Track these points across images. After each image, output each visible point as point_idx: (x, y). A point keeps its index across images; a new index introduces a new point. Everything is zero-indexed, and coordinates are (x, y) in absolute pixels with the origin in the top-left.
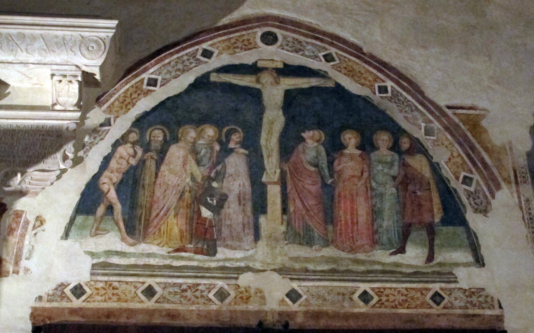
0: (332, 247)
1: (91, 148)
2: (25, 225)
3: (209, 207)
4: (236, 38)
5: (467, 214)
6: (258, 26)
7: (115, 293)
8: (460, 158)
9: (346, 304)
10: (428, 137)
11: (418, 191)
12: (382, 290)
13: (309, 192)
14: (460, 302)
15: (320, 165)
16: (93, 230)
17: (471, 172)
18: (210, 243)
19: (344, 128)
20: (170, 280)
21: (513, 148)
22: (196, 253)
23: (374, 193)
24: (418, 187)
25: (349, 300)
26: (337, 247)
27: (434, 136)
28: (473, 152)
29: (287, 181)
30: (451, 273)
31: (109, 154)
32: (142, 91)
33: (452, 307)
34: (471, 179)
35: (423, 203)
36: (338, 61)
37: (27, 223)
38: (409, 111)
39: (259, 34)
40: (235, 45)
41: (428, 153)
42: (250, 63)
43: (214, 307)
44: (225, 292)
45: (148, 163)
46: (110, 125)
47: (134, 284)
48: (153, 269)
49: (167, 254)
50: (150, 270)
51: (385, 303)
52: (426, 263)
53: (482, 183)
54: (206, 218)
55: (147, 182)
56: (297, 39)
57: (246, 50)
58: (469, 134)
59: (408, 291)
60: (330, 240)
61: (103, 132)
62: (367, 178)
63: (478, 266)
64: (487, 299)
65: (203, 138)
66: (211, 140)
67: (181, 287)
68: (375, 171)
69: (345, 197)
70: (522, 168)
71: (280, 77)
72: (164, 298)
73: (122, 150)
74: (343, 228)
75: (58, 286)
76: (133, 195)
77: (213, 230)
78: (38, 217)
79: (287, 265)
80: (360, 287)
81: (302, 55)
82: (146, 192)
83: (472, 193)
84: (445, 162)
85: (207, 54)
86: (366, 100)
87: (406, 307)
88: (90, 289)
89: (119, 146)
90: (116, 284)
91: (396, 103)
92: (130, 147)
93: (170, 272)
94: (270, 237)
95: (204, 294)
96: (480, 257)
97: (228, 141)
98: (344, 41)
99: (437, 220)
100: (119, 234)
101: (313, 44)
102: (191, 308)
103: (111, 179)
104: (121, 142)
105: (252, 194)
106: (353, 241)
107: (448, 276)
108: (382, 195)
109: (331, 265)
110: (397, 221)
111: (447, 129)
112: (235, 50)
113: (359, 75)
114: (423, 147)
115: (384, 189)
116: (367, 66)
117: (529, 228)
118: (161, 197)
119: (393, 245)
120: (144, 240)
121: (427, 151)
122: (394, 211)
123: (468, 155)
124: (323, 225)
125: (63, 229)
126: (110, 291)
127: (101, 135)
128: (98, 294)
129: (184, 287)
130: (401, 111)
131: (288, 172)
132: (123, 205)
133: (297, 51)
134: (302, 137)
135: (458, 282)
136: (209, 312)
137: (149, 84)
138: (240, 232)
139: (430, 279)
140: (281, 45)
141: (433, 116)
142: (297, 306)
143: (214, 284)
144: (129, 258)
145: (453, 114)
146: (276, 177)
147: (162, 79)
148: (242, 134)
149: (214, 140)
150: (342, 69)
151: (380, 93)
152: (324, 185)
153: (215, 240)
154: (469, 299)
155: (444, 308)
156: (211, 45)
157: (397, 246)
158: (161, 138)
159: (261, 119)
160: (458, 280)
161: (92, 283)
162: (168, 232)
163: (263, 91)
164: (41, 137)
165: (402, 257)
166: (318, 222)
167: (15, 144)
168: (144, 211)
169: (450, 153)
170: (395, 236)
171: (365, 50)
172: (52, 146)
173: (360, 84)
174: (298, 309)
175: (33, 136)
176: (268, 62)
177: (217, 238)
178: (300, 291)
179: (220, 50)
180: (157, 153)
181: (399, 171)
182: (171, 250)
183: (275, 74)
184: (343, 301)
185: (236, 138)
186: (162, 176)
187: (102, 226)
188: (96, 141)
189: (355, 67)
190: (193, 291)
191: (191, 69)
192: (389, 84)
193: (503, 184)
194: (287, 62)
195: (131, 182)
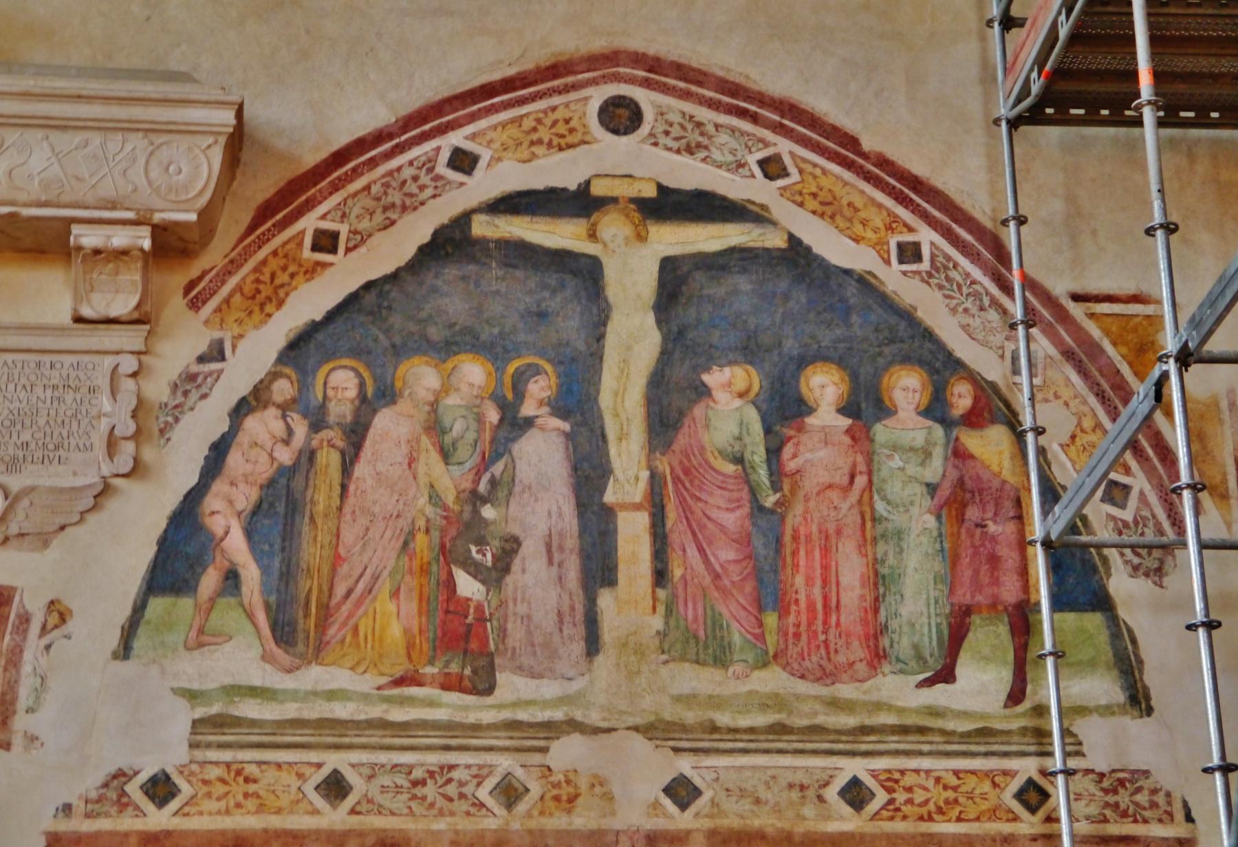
0: (777, 669)
1: (177, 420)
2: (21, 623)
3: (475, 570)
5: (1111, 580)
6: (594, 82)
7: (250, 792)
9: (809, 811)
11: (990, 523)
12: (897, 776)
13: (722, 528)
14: (1087, 805)
15: (747, 456)
16: (193, 634)
18: (482, 662)
20: (383, 757)
22: (445, 687)
24: (990, 515)
25: (817, 802)
31: (223, 435)
32: (300, 265)
34: (1126, 489)
36: (795, 177)
37: (25, 619)
38: (974, 310)
39: (594, 106)
40: (535, 137)
42: (573, 187)
43: (491, 823)
44: (517, 785)
46: (223, 359)
47: (295, 767)
48: (344, 732)
49: (375, 692)
50: (333, 732)
51: (903, 808)
52: (1006, 706)
53: (1153, 498)
54: (469, 599)
55: (321, 507)
56: (691, 117)
57: (561, 149)
59: (959, 778)
60: (771, 653)
61: (206, 378)
62: (864, 491)
63: (1136, 713)
64: (1155, 798)
65: (457, 390)
66: (476, 397)
67: (410, 773)
68: (884, 472)
69: (808, 538)
71: (648, 222)
72: (370, 801)
74: (804, 618)
75: (109, 778)
76: (287, 544)
77: (485, 629)
78: (52, 602)
79: (667, 716)
80: (841, 769)
81: (704, 160)
82: (320, 533)
83: (1126, 524)
84: (1062, 446)
85: (463, 161)
87: (954, 818)
88: (189, 782)
89: (246, 415)
90: (251, 770)
91: (941, 287)
92: (276, 418)
93: (385, 736)
94: (625, 645)
95: (467, 790)
96: (1141, 691)
98: (813, 121)
101: (733, 130)
103: (231, 503)
104: (254, 403)
105: (581, 536)
106: (828, 653)
108: (899, 534)
109: (773, 713)
110: (936, 602)
111: (1068, 355)
112: (534, 149)
113: (848, 212)
118: (357, 548)
119: (926, 662)
120: (317, 657)
122: (931, 577)
124: (755, 612)
125: (118, 633)
126: (239, 788)
127: (199, 386)
128: (209, 795)
129: (418, 774)
130: (954, 311)
131: (669, 478)
132: (265, 570)
133: (690, 150)
135: (1084, 755)
137: (315, 248)
138: (551, 634)
139: (1014, 748)
140: (651, 135)
142: (691, 818)
143: (491, 766)
144: (282, 702)
145: (1086, 314)
146: (638, 492)
147: (350, 231)
148: (554, 380)
149: (484, 395)
150: (807, 197)
151: (901, 262)
153: (491, 655)
154: (1111, 799)
156: (473, 137)
157: (936, 664)
158: (352, 393)
159: (600, 338)
160: (1085, 749)
161: (194, 767)
162: (377, 636)
163: (604, 260)
164: (49, 392)
165: (946, 691)
166: (744, 608)
168: (315, 582)
169: (1075, 421)
170: (930, 638)
171: (867, 144)
172: (79, 416)
173: (850, 238)
174: (690, 826)
175: (29, 388)
176: (617, 181)
177: (497, 648)
178: (697, 781)
179: (496, 151)
180: (344, 433)
181: (945, 471)
182: (384, 680)
183: (637, 216)
184: (803, 804)
188: (190, 403)
190: (441, 781)
191: (422, 204)
192: (926, 237)
194: (665, 182)
195: (281, 508)
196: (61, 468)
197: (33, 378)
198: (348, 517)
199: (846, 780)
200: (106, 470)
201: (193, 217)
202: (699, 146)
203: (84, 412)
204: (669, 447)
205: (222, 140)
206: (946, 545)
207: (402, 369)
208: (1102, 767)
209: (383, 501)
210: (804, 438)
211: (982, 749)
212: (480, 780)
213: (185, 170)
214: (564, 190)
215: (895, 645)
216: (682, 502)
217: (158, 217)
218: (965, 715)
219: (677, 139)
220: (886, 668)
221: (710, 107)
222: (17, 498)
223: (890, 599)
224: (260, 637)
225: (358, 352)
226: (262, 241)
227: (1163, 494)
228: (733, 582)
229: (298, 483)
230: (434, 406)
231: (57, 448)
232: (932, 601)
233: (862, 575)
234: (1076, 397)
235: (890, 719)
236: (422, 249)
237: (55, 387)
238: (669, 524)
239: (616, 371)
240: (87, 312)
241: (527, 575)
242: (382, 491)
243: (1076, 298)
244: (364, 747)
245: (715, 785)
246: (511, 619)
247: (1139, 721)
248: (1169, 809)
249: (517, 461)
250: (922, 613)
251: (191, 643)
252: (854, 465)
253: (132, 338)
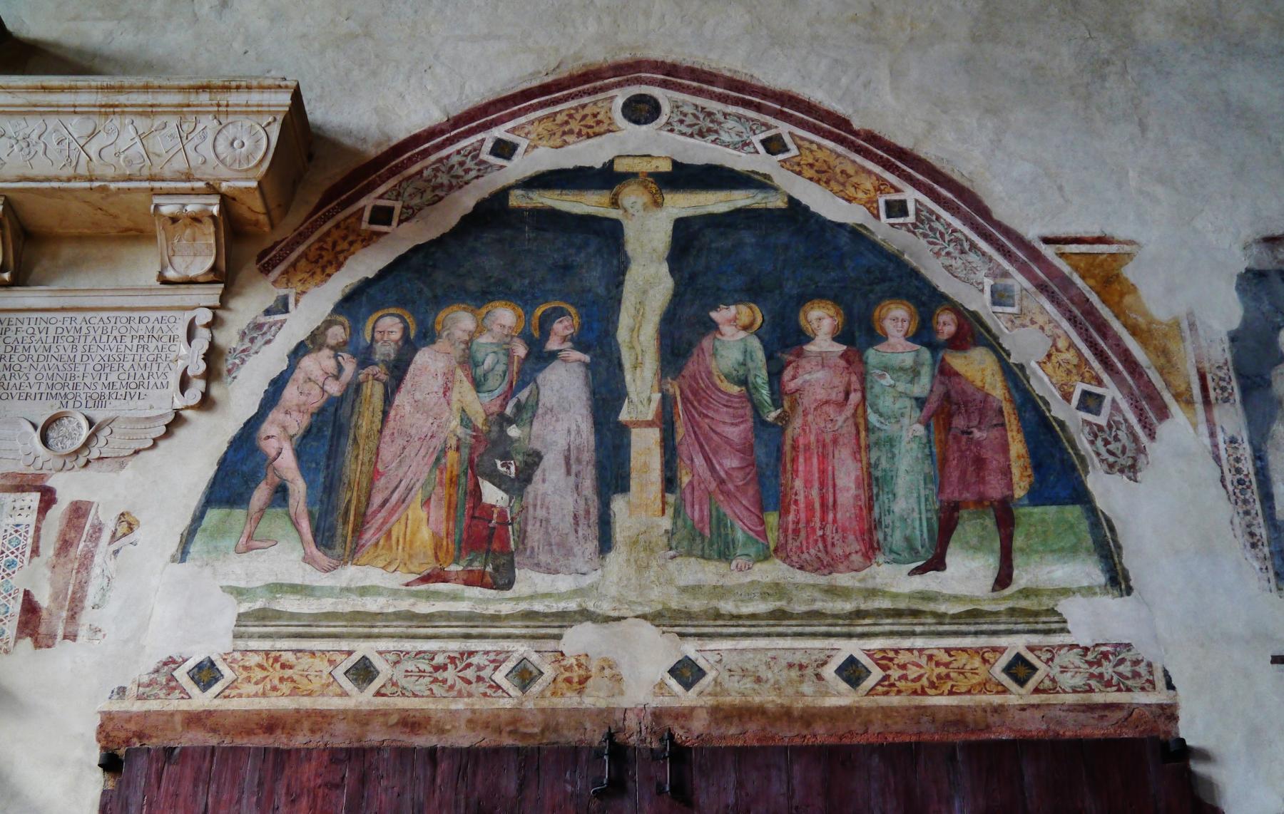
0: (778, 561)
1: (243, 361)
2: (95, 532)
4: (567, 112)
6: (619, 85)
7: (286, 677)
8: (1072, 352)
9: (807, 688)
11: (975, 430)
12: (891, 654)
13: (728, 441)
14: (1073, 677)
15: (751, 379)
16: (243, 540)
17: (1100, 383)
18: (502, 560)
19: (803, 299)
20: (408, 645)
21: (1198, 323)
22: (468, 583)
24: (975, 423)
25: (815, 680)
26: (786, 559)
27: (1013, 306)
28: (1104, 337)
29: (675, 418)
30: (1052, 612)
32: (359, 235)
33: (1054, 688)
34: (1100, 398)
35: (987, 454)
36: (794, 151)
37: (98, 529)
38: (956, 253)
39: (619, 102)
40: (566, 128)
41: (1000, 345)
42: (598, 165)
43: (506, 703)
44: (532, 668)
45: (366, 390)
46: (287, 311)
47: (328, 655)
49: (404, 588)
50: (365, 624)
51: (898, 683)
52: (994, 590)
53: (1124, 405)
54: (494, 506)
55: (363, 430)
56: (703, 108)
57: (589, 137)
58: (1094, 299)
59: (950, 656)
60: (772, 547)
61: (270, 327)
62: (858, 406)
63: (1116, 593)
64: (1137, 668)
66: (507, 336)
67: (433, 659)
68: (877, 389)
69: (807, 448)
70: (1219, 367)
71: (664, 191)
72: (394, 684)
74: (803, 515)
75: (160, 665)
76: (331, 462)
78: (123, 514)
81: (713, 142)
83: (1100, 428)
84: (1039, 363)
85: (504, 150)
86: (857, 234)
87: (946, 692)
88: (231, 668)
89: (303, 356)
90: (288, 657)
91: (925, 236)
93: (410, 627)
94: (635, 543)
97: (545, 333)
98: (809, 107)
99: (1019, 492)
100: (299, 546)
101: (739, 117)
102: (453, 707)
103: (284, 428)
104: (311, 346)
105: (597, 448)
107: (1044, 619)
108: (891, 442)
110: (927, 500)
111: (1042, 288)
114: (988, 330)
115: (896, 427)
116: (859, 159)
117: (1236, 503)
119: (918, 552)
120: (353, 558)
121: (996, 338)
123: (1093, 346)
124: (757, 512)
125: (178, 539)
126: (277, 673)
127: (265, 333)
128: (248, 679)
129: (440, 659)
130: (937, 254)
131: (679, 398)
132: (310, 485)
133: (701, 134)
134: (712, 320)
135: (1069, 632)
136: (496, 714)
139: (1002, 627)
140: (668, 123)
141: (1010, 261)
142: (695, 696)
144: (319, 598)
146: (650, 413)
147: (403, 207)
148: (576, 320)
151: (889, 216)
152: (760, 422)
154: (1095, 670)
155: (1037, 691)
156: (513, 130)
157: (926, 555)
158: (397, 335)
159: (620, 285)
160: (1069, 626)
161: (237, 655)
162: (408, 539)
163: (625, 222)
164: (136, 342)
165: (937, 578)
166: (747, 509)
167: (78, 359)
168: (355, 494)
169: (1051, 343)
170: (921, 531)
171: (856, 125)
172: (159, 360)
173: (843, 198)
174: (693, 704)
175: (119, 340)
176: (637, 160)
177: (517, 548)
178: (702, 663)
179: (532, 140)
180: (388, 368)
181: (932, 387)
183: (654, 187)
184: (801, 682)
185: (562, 327)
186: (398, 417)
187: (263, 527)
188: (255, 348)
189: (833, 161)
190: (460, 666)
191: (467, 183)
192: (911, 195)
193: (1174, 407)
194: (679, 160)
195: (328, 432)
196: (140, 402)
197: (123, 330)
198: (387, 439)
199: (843, 659)
200: (179, 404)
202: (709, 130)
203: (164, 358)
204: (680, 372)
205: (280, 118)
206: (935, 450)
208: (1086, 641)
209: (422, 425)
210: (803, 362)
211: (972, 628)
212: (497, 664)
213: (246, 144)
214: (591, 168)
215: (889, 538)
216: (691, 419)
217: (224, 186)
218: (956, 598)
219: (690, 126)
220: (881, 558)
221: (719, 100)
222: (99, 428)
223: (884, 497)
224: (302, 541)
225: (402, 303)
227: (1134, 402)
228: (737, 487)
229: (346, 408)
231: (138, 387)
232: (923, 500)
233: (857, 478)
234: (1050, 322)
235: (886, 604)
236: (465, 219)
237: (141, 337)
238: (678, 438)
239: (632, 311)
240: (171, 274)
241: (546, 485)
242: (418, 415)
243: (1047, 241)
244: (391, 636)
245: (718, 667)
246: (530, 522)
247: (1119, 600)
248: (1151, 678)
249: (541, 387)
250: (913, 510)
251: (241, 547)
252: (849, 384)
253: (211, 295)
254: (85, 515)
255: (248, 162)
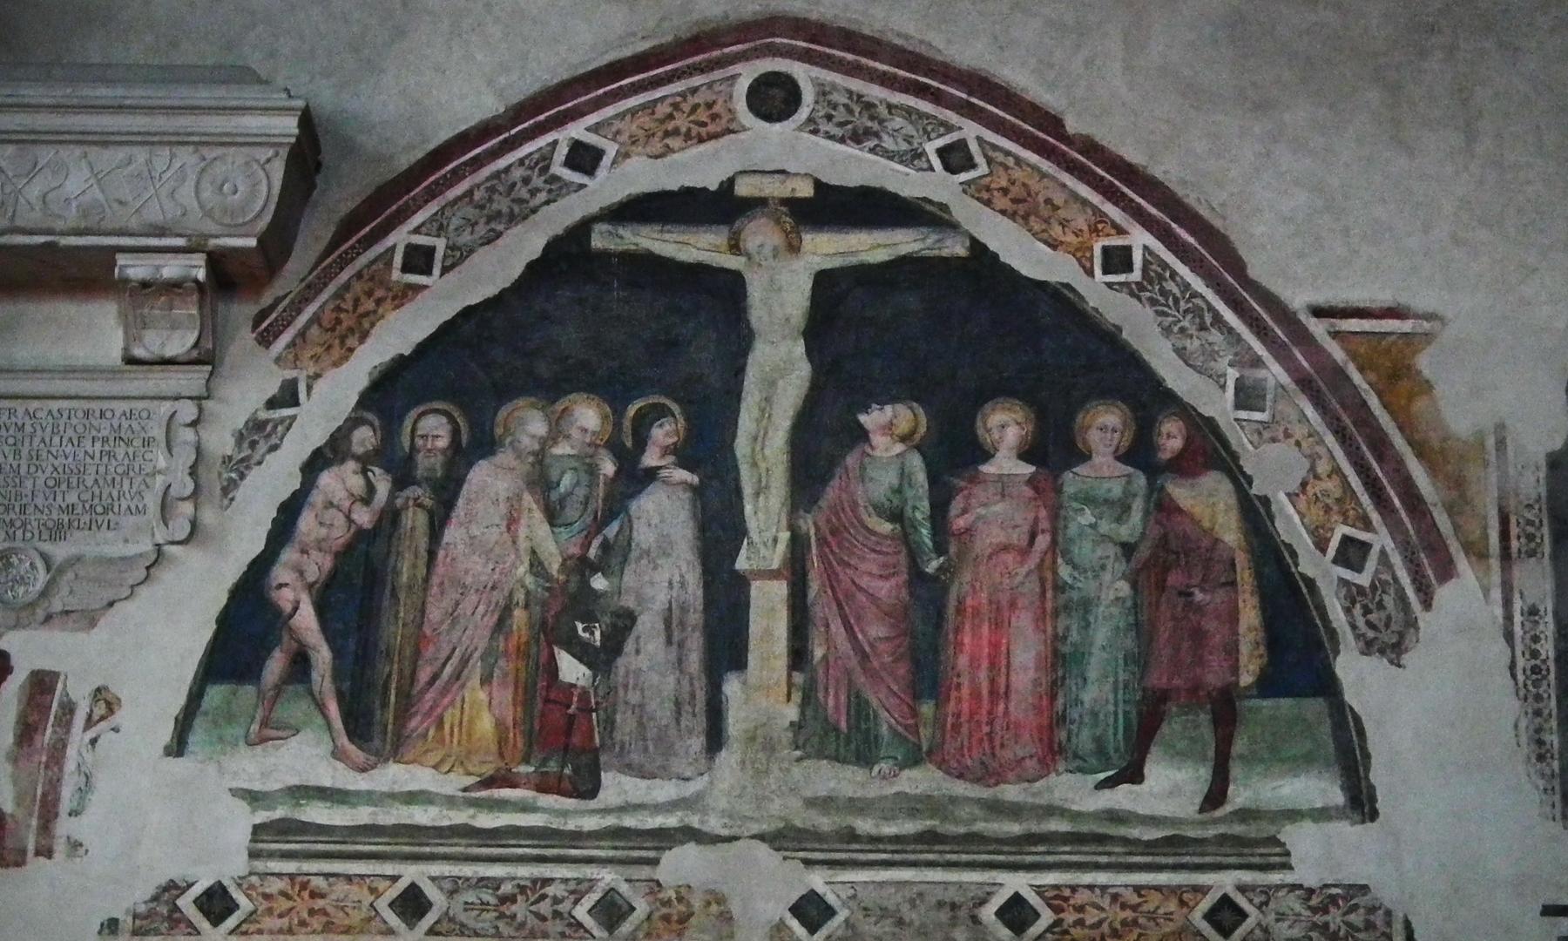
1: (242, 476)
2: (64, 714)
3: (583, 653)
4: (670, 101)
5: (1339, 659)
8: (1336, 479)
10: (1243, 414)
11: (1196, 591)
12: (1067, 893)
13: (872, 597)
14: (1290, 927)
15: (908, 511)
16: (255, 727)
17: (1367, 525)
18: (584, 759)
20: (467, 870)
21: (1508, 441)
22: (543, 788)
23: (1062, 599)
25: (970, 924)
26: (942, 765)
27: (1263, 410)
28: (1380, 459)
29: (809, 564)
30: (1274, 841)
31: (294, 494)
32: (389, 289)
34: (1365, 547)
35: (1210, 625)
37: (69, 709)
38: (1193, 331)
39: (743, 85)
40: (670, 126)
41: (1240, 468)
42: (713, 187)
44: (620, 902)
46: (296, 403)
47: (368, 881)
48: (425, 840)
49: (461, 794)
51: (1072, 931)
52: (1201, 811)
53: (1396, 559)
54: (573, 686)
55: (404, 578)
56: (860, 96)
57: (701, 140)
58: (1374, 402)
59: (1140, 896)
61: (275, 427)
62: (1046, 553)
63: (1357, 817)
65: (568, 437)
66: (589, 445)
67: (498, 888)
68: (1073, 530)
69: (977, 612)
70: (1529, 506)
71: (801, 228)
72: (451, 920)
73: (327, 480)
74: (965, 707)
77: (590, 720)
78: (98, 690)
79: (798, 823)
80: (1001, 885)
81: (872, 150)
82: (402, 609)
83: (1361, 590)
84: (1288, 495)
85: (584, 158)
86: (1060, 298)
88: (248, 896)
90: (318, 883)
92: (355, 473)
93: (471, 845)
94: (753, 739)
95: (563, 908)
96: (1365, 791)
97: (641, 443)
99: (1246, 679)
100: (326, 738)
101: (909, 112)
103: (301, 573)
106: (993, 748)
107: (1262, 850)
108: (1086, 605)
109: (924, 819)
110: (1126, 687)
112: (669, 141)
113: (1045, 211)
115: (1093, 585)
117: (1526, 699)
118: (445, 627)
119: (1108, 758)
121: (1235, 457)
122: (1121, 656)
124: (908, 700)
126: (302, 905)
127: (269, 436)
128: (270, 911)
129: (507, 888)
130: (1167, 331)
132: (337, 653)
133: (857, 138)
134: (860, 426)
135: (1291, 868)
138: (666, 726)
140: (810, 120)
141: (1264, 342)
143: (591, 880)
144: (354, 806)
145: (1329, 333)
146: (776, 557)
147: (447, 247)
148: (682, 422)
149: (598, 442)
150: (995, 193)
151: (1106, 271)
152: (917, 576)
153: (595, 752)
154: (1319, 919)
158: (442, 443)
159: (740, 371)
160: (1293, 861)
161: (254, 879)
163: (748, 276)
164: (98, 445)
165: (1131, 792)
167: (23, 470)
168: (396, 666)
169: (1307, 464)
170: (1116, 729)
171: (1072, 125)
172: (131, 474)
173: (1046, 242)
175: (76, 443)
176: (767, 179)
178: (831, 899)
182: (470, 781)
185: (663, 434)
186: (448, 560)
187: (281, 712)
188: (257, 457)
189: (1034, 184)
191: (534, 211)
192: (1140, 239)
193: (1462, 563)
194: (824, 180)
196: (110, 534)
197: (80, 429)
198: (435, 590)
199: (1007, 897)
201: (252, 242)
202: (868, 133)
203: (137, 469)
204: (816, 502)
205: (284, 152)
207: (502, 414)
208: (1311, 881)
209: (476, 569)
210: (978, 491)
211: (1170, 860)
213: (241, 188)
214: (705, 190)
215: (1074, 740)
217: (213, 242)
218: (1153, 821)
219: (841, 125)
220: (1061, 766)
221: (882, 84)
222: (61, 571)
225: (452, 393)
226: (344, 262)
227: (1409, 554)
228: (883, 663)
230: (540, 457)
231: (106, 511)
232: (1121, 686)
233: (1038, 654)
234: (1310, 435)
235: (1062, 826)
236: (531, 267)
237: (105, 440)
238: (812, 594)
239: (756, 413)
240: (139, 352)
241: (641, 656)
242: (475, 558)
245: (851, 903)
246: (621, 707)
247: (1359, 828)
248: (1388, 931)
249: (635, 522)
250: (1107, 701)
252: (1036, 520)
253: (191, 380)
254: (51, 690)
255: (244, 217)
